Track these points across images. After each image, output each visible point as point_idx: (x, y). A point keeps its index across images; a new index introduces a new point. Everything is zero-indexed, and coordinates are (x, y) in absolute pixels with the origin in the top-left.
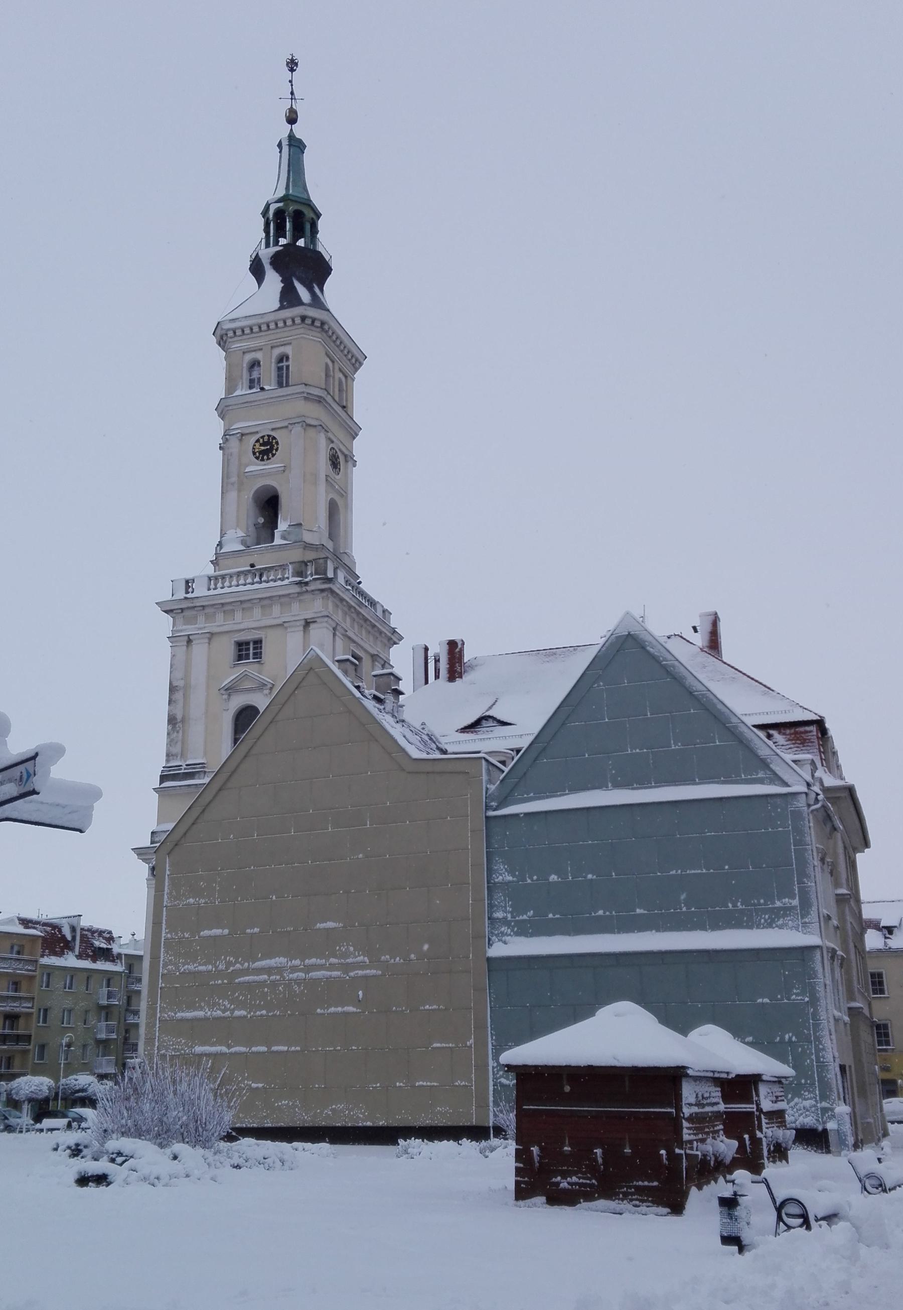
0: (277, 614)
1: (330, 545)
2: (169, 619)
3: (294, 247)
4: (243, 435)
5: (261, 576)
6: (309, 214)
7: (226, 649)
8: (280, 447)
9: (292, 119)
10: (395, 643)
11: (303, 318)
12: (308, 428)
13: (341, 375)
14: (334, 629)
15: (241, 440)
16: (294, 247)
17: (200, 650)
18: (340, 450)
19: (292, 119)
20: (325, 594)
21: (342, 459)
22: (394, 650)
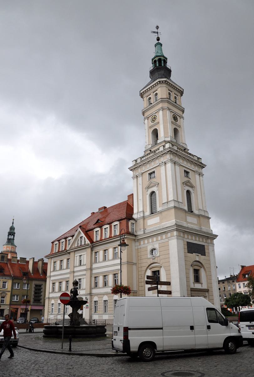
0: (157, 162)
1: (175, 141)
2: (131, 172)
3: (160, 68)
4: (148, 118)
5: (155, 152)
6: (162, 58)
7: (147, 175)
8: (157, 117)
9: (158, 39)
10: (204, 167)
11: (160, 81)
12: (164, 110)
14: (175, 163)
15: (148, 119)
16: (160, 68)
17: (140, 179)
18: (177, 115)
19: (158, 39)
20: (169, 152)
21: (178, 117)
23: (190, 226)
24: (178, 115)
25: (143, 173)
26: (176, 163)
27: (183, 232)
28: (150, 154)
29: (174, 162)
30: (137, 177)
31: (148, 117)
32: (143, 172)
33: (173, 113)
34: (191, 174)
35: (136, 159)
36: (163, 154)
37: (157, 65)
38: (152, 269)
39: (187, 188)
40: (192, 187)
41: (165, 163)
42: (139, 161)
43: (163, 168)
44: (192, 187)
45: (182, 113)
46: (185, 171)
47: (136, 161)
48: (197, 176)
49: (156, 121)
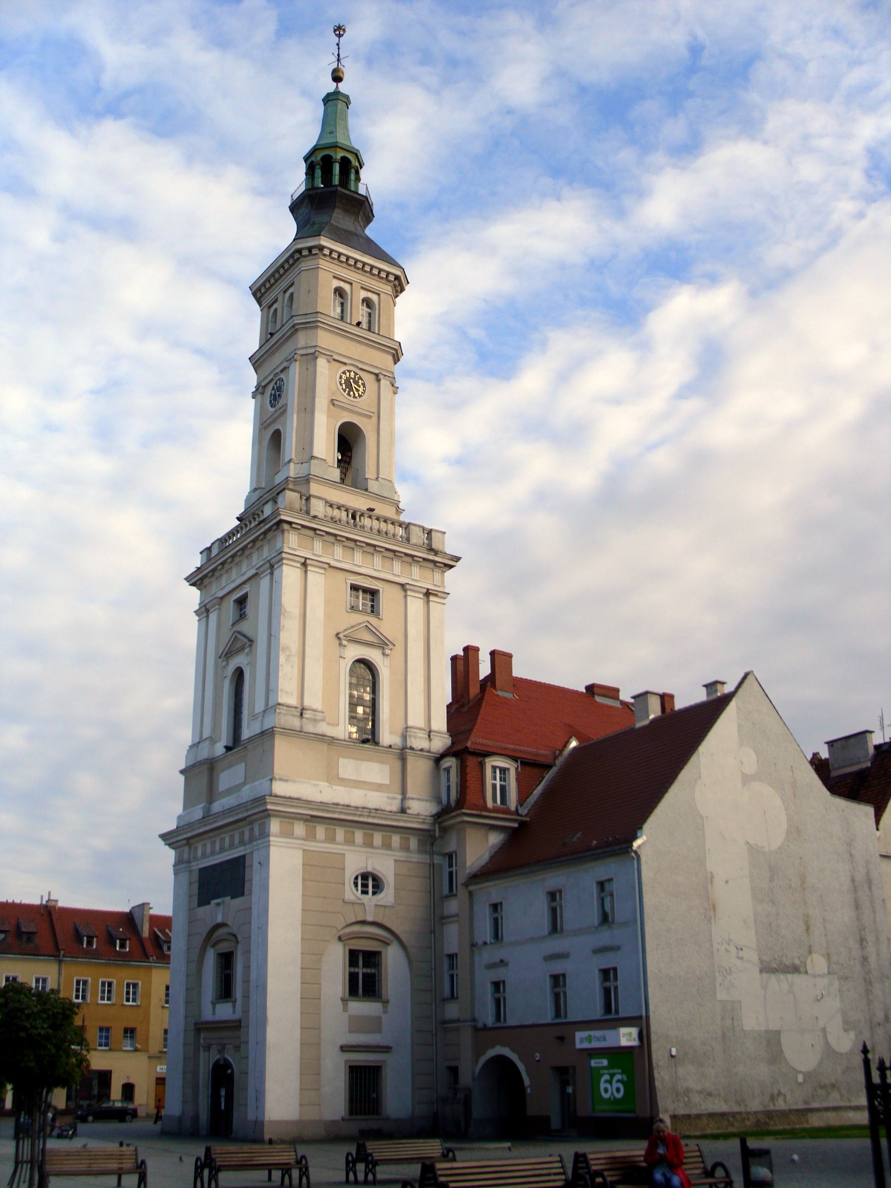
10: (451, 567)
13: (364, 294)
22: (449, 574)
23: (356, 797)
24: (361, 369)
25: (222, 598)
26: (308, 562)
27: (306, 821)
28: (242, 528)
29: (303, 560)
30: (207, 611)
31: (263, 384)
32: (221, 594)
33: (345, 364)
34: (388, 597)
35: (208, 546)
36: (265, 533)
37: (336, 180)
38: (218, 947)
39: (355, 652)
40: (383, 644)
41: (272, 567)
42: (215, 552)
43: (265, 582)
44: (383, 644)
45: (390, 358)
46: (355, 588)
47: (209, 549)
48: (416, 605)
49: (282, 402)
